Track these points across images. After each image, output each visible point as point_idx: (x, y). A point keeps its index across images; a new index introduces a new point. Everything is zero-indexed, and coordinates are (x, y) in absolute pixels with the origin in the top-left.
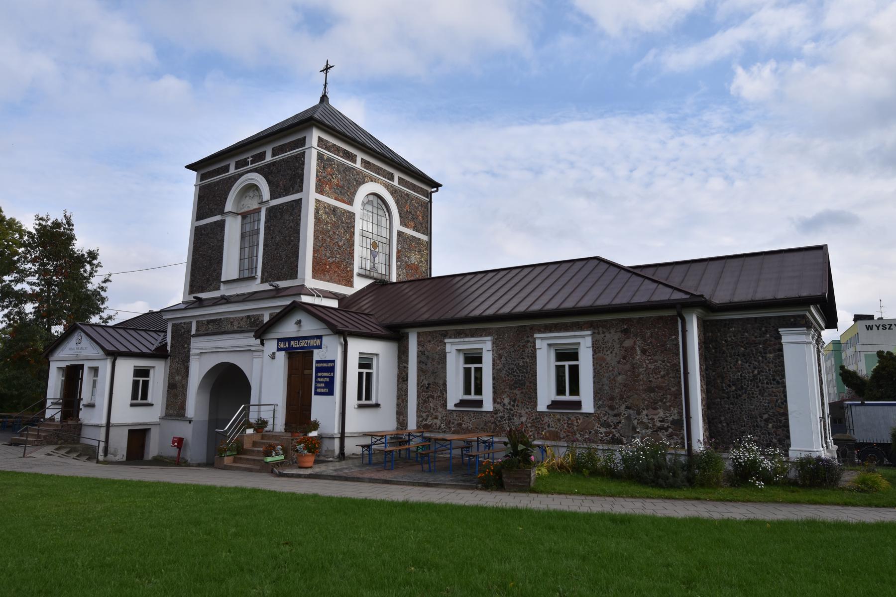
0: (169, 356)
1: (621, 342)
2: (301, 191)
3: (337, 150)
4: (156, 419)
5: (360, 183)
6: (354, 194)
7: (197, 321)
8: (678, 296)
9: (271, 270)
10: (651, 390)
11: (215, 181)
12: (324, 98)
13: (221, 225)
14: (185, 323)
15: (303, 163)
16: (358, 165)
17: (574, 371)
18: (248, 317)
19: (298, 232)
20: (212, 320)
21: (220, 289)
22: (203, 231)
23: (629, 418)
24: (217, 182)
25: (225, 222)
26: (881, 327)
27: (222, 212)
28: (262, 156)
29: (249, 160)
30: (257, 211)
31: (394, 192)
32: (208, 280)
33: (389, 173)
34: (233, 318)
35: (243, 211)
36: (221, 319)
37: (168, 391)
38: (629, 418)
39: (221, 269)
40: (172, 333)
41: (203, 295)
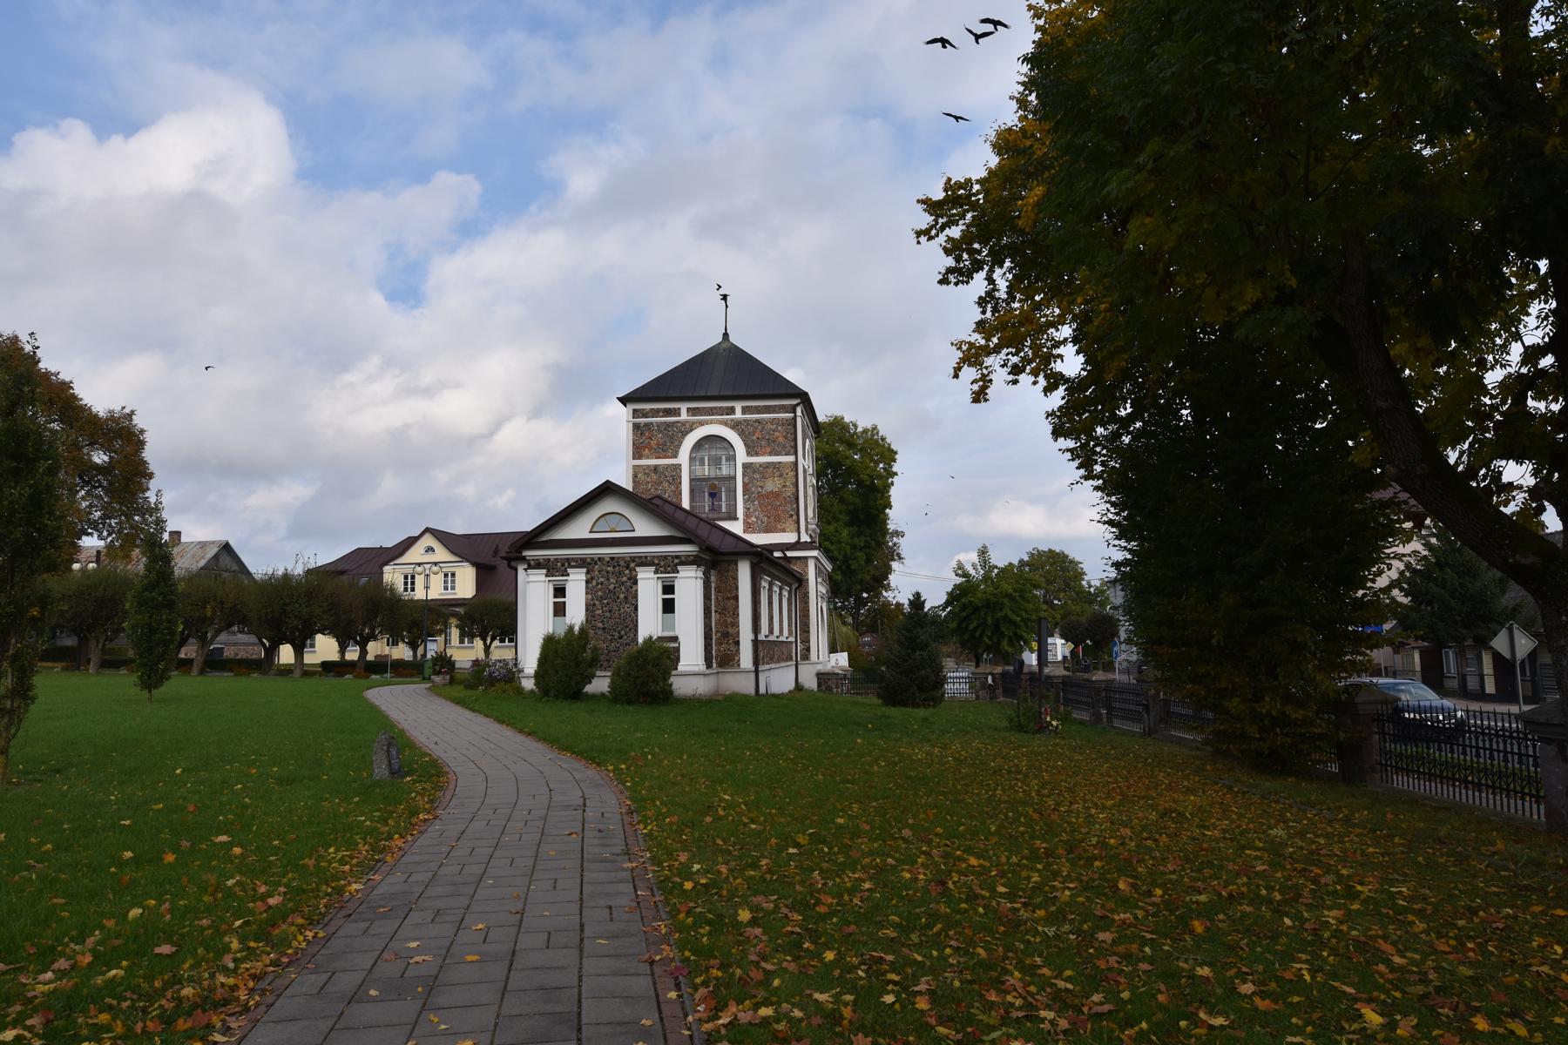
3: (655, 413)
5: (685, 434)
6: (679, 446)
12: (726, 335)
16: (684, 416)
31: (735, 426)
33: (727, 408)
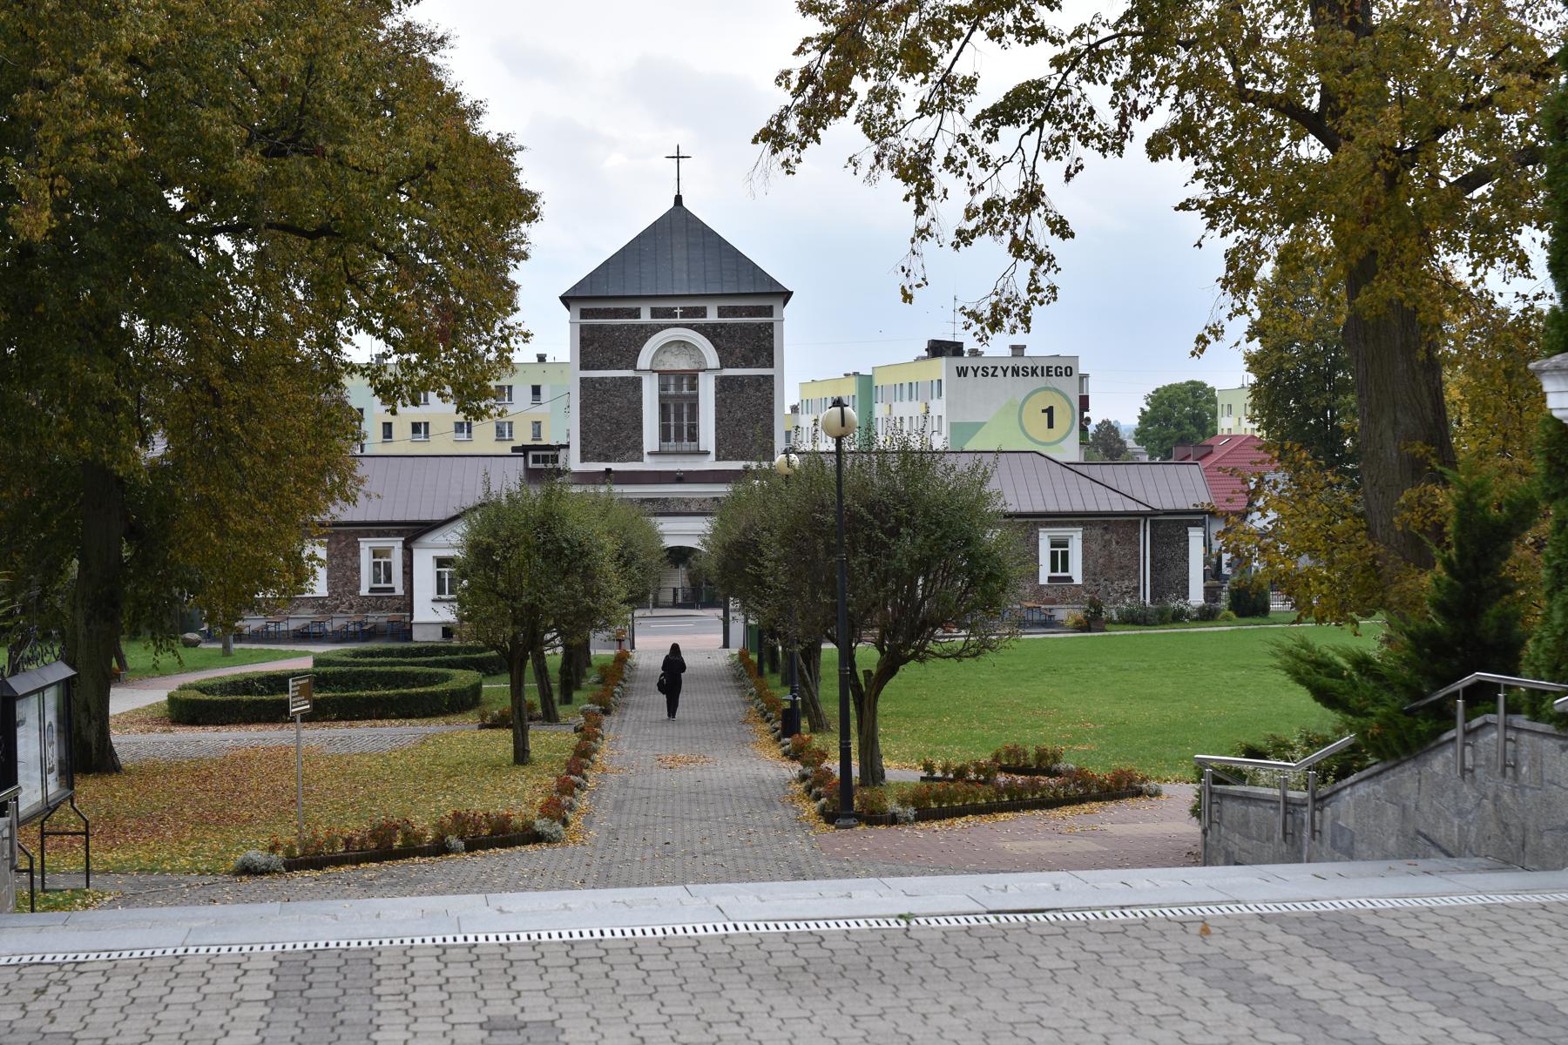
1: (1102, 536)
2: (772, 366)
8: (1143, 508)
10: (1121, 568)
12: (678, 199)
13: (636, 384)
15: (772, 336)
17: (1065, 555)
23: (1106, 587)
26: (980, 372)
27: (632, 365)
28: (702, 312)
29: (678, 311)
32: (616, 448)
35: (662, 368)
38: (1106, 587)
39: (641, 436)
41: (616, 466)
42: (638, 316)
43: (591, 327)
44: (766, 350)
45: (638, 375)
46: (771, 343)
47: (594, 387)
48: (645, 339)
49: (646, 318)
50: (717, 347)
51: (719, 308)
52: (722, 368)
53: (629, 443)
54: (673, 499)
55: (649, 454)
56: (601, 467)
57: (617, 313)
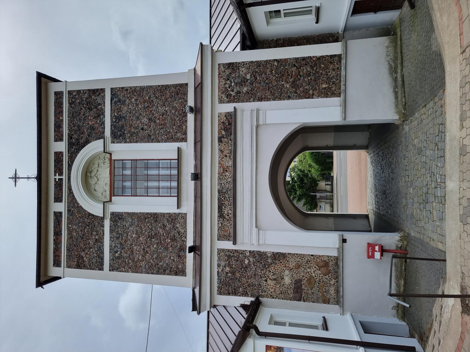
0: (257, 299)
2: (103, 90)
4: (348, 316)
7: (218, 240)
9: (174, 127)
11: (66, 237)
14: (219, 266)
15: (79, 92)
18: (220, 141)
19: (142, 89)
20: (219, 206)
21: (186, 213)
22: (117, 255)
24: (68, 234)
25: (113, 213)
28: (58, 155)
29: (57, 177)
30: (113, 178)
32: (174, 239)
34: (220, 167)
35: (108, 193)
36: (219, 192)
37: (304, 301)
39: (163, 215)
40: (229, 294)
42: (61, 213)
43: (69, 257)
44: (90, 96)
45: (108, 216)
46: (84, 92)
47: (119, 258)
48: (80, 208)
49: (61, 207)
50: (87, 142)
51: (56, 140)
52: (103, 138)
53: (169, 226)
54: (220, 184)
55: (179, 206)
56: (190, 257)
57: (58, 233)
